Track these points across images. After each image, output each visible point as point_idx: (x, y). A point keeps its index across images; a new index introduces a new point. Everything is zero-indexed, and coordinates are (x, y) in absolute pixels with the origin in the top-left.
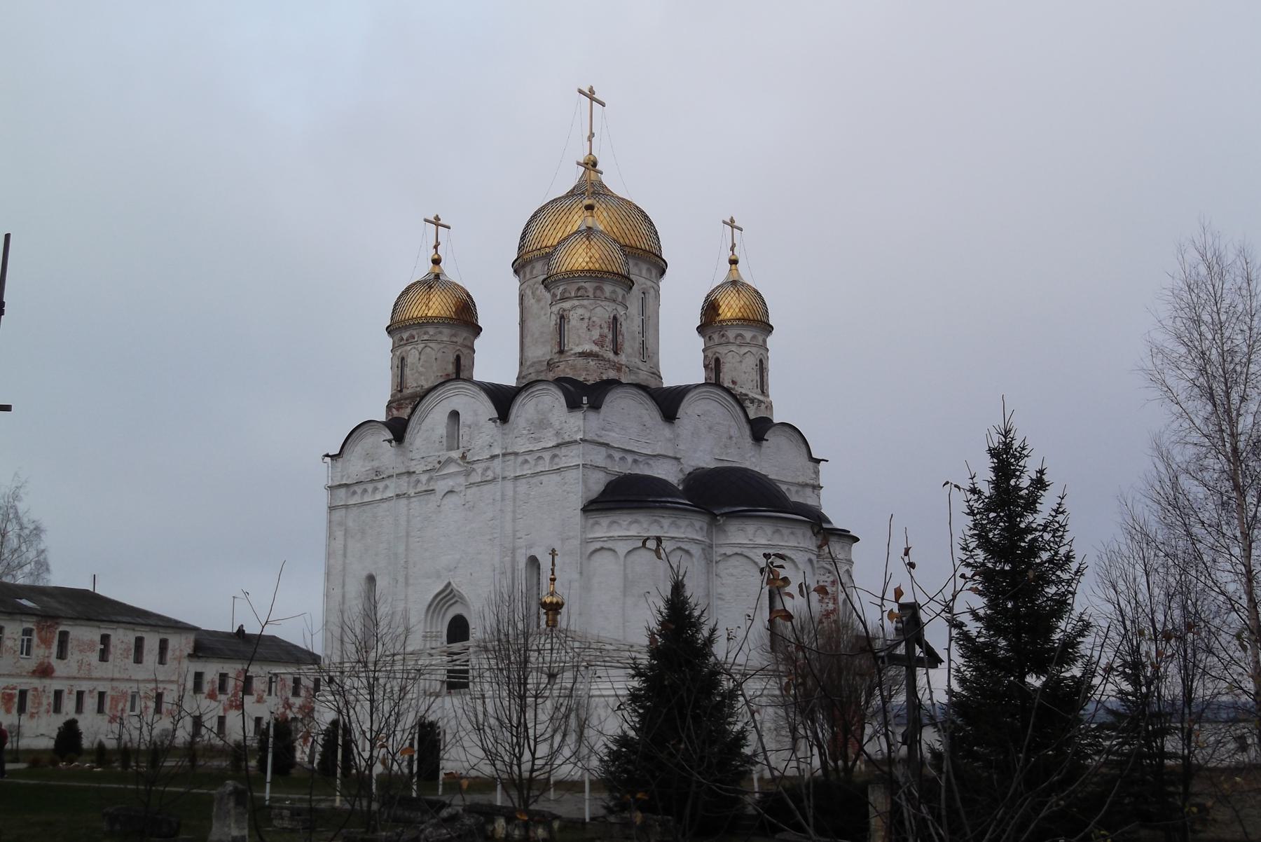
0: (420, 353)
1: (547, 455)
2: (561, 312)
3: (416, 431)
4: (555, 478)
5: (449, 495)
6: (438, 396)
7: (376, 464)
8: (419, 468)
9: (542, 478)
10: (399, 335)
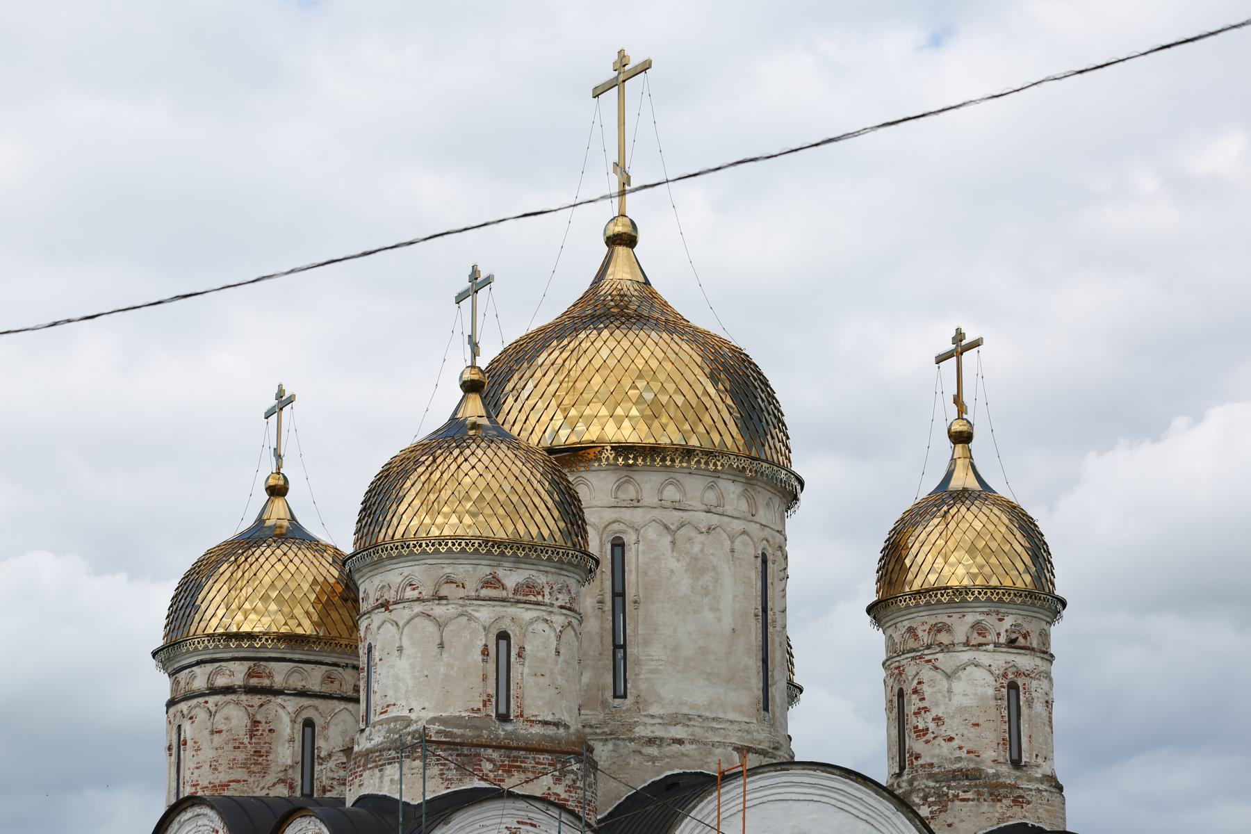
0: (559, 638)
2: (1010, 676)
10: (488, 570)
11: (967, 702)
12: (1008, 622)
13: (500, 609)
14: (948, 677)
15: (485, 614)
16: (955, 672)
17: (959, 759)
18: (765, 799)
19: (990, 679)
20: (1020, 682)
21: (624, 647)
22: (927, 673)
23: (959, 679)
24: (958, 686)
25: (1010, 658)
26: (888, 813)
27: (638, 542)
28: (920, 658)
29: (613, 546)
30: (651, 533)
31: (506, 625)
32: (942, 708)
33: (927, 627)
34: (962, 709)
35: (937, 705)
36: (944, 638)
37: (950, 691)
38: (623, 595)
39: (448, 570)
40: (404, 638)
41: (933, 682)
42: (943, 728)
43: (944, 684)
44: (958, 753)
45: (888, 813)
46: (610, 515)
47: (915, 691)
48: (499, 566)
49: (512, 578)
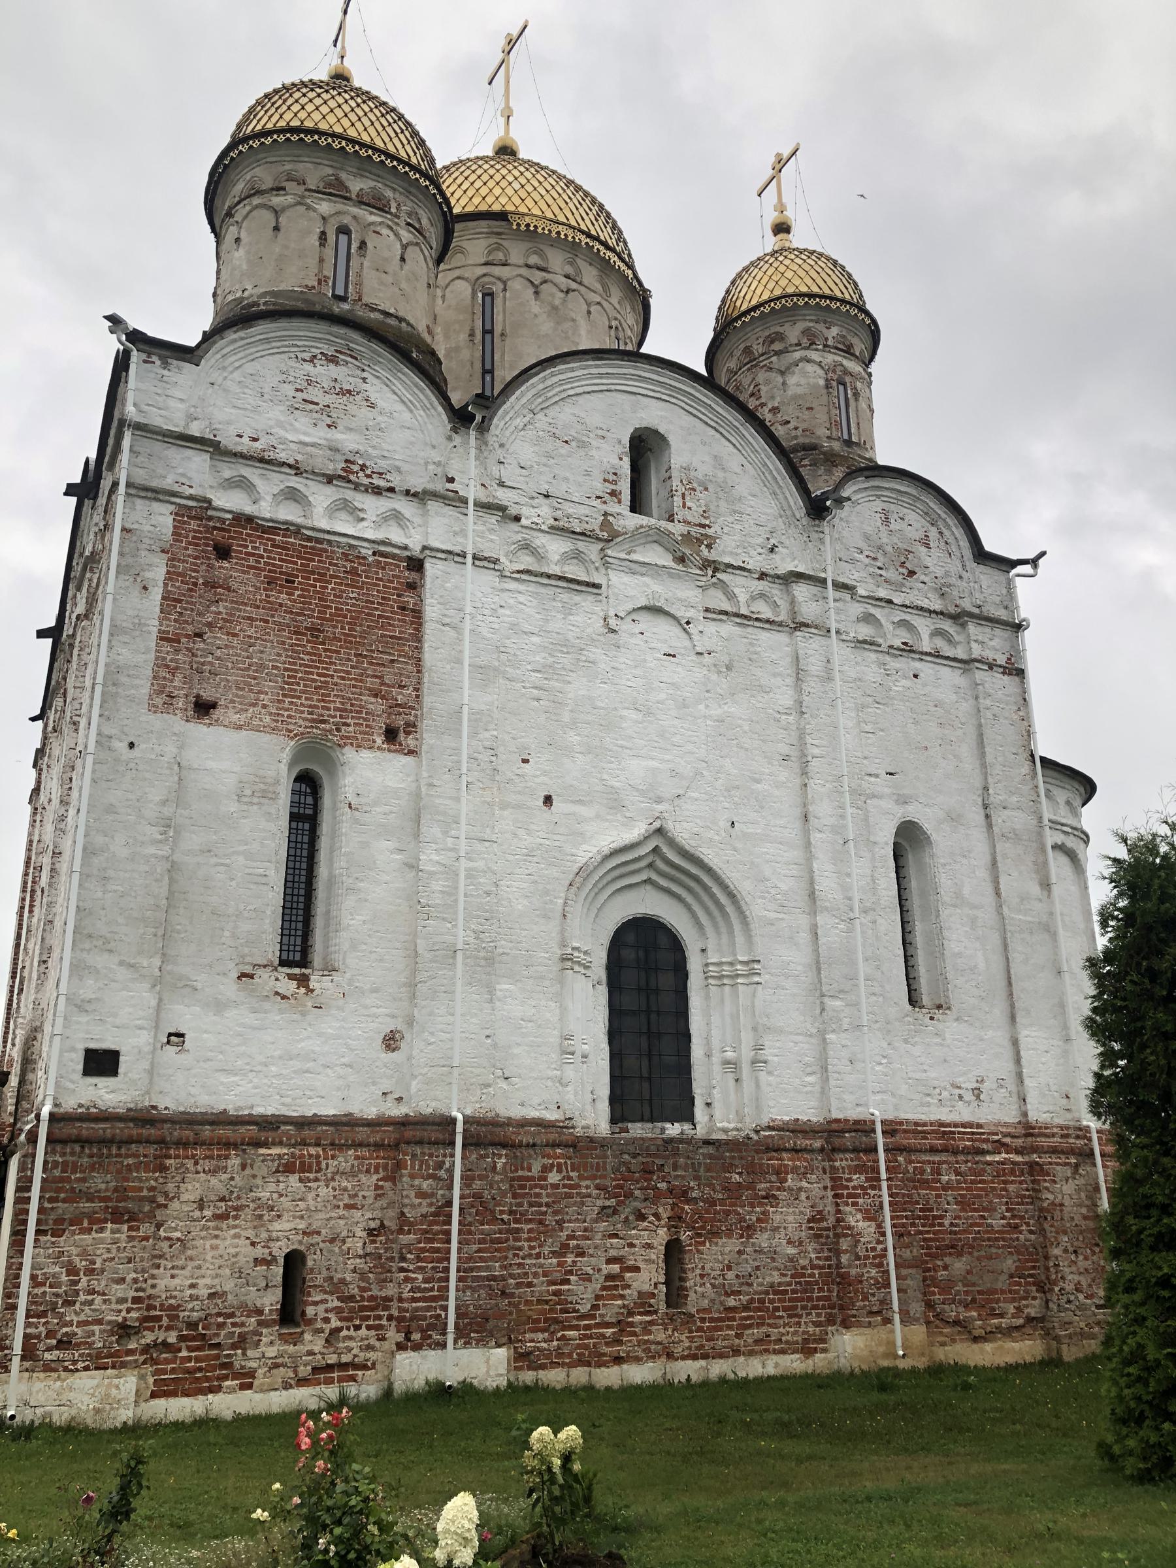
0: (405, 247)
1: (924, 626)
3: (519, 422)
4: (950, 676)
5: (644, 617)
6: (601, 376)
7: (349, 441)
8: (537, 513)
9: (918, 665)
10: (330, 171)
11: (799, 391)
12: (835, 331)
13: (340, 207)
14: (782, 373)
15: (325, 207)
16: (788, 368)
17: (796, 437)
18: (613, 387)
19: (821, 372)
20: (848, 379)
21: (491, 372)
22: (761, 376)
23: (794, 373)
24: (792, 380)
25: (840, 359)
26: (736, 424)
27: (505, 290)
28: (755, 366)
29: (484, 295)
30: (516, 285)
31: (346, 220)
32: (778, 399)
33: (761, 340)
34: (795, 397)
35: (773, 398)
36: (777, 346)
37: (784, 383)
38: (491, 332)
39: (288, 167)
40: (243, 231)
41: (768, 382)
42: (779, 415)
43: (780, 379)
44: (794, 433)
45: (736, 424)
46: (481, 271)
47: (752, 395)
48: (341, 169)
49: (356, 185)
